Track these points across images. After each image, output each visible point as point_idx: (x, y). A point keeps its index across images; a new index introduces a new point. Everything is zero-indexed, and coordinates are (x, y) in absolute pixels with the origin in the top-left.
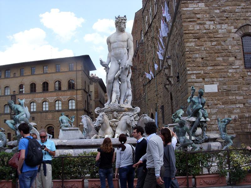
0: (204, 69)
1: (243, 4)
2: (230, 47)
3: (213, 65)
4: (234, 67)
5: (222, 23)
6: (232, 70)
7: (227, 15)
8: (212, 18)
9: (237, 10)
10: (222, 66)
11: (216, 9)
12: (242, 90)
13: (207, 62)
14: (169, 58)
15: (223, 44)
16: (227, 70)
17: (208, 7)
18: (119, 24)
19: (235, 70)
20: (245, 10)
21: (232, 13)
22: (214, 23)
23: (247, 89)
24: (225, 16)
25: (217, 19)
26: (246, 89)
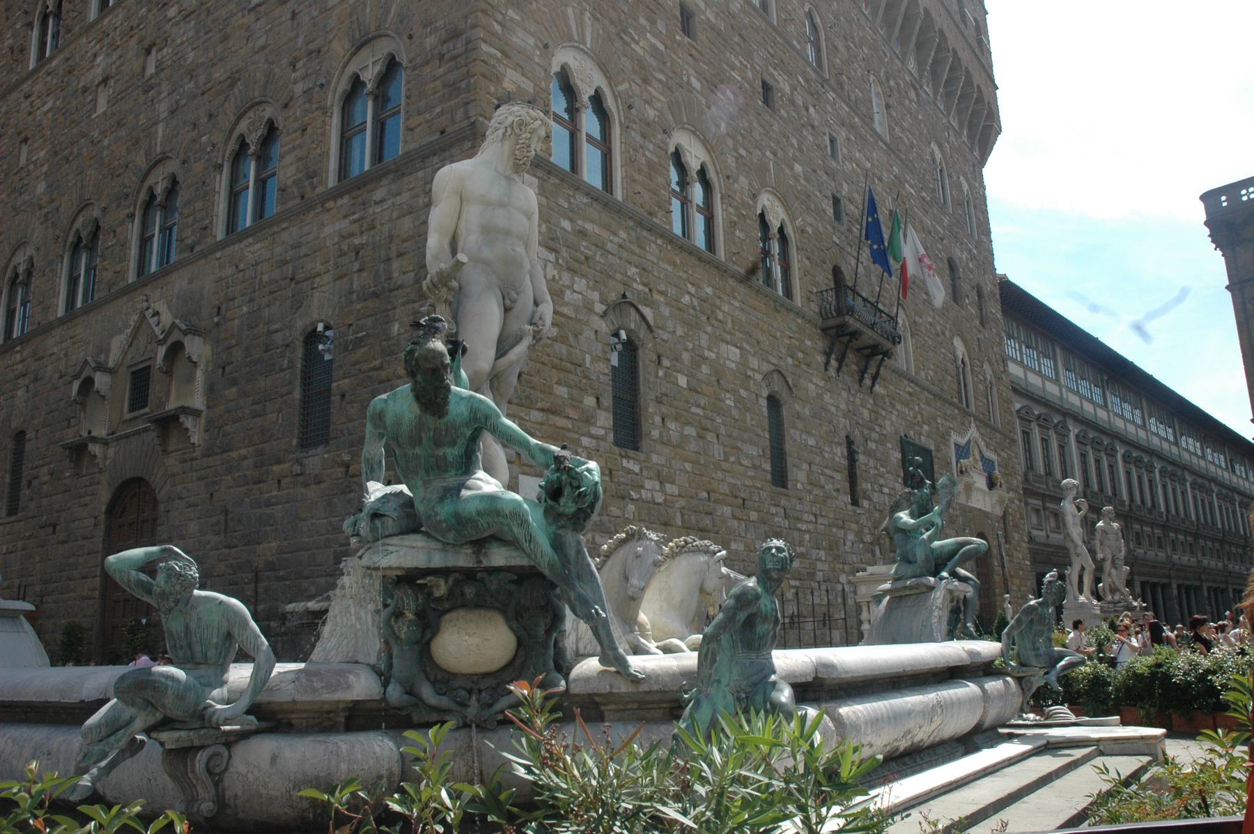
0: (522, 415)
1: (623, 234)
2: (588, 357)
3: (547, 406)
4: (593, 431)
5: (575, 272)
6: (589, 440)
7: (586, 248)
8: (552, 239)
9: (609, 246)
10: (567, 417)
11: (566, 217)
12: (608, 515)
13: (532, 392)
14: (193, 331)
15: (573, 343)
16: (576, 436)
17: (546, 197)
18: (529, 135)
19: (594, 441)
20: (625, 255)
21: (597, 246)
22: (557, 259)
23: (620, 515)
24: (583, 249)
25: (564, 249)
26: (618, 513)
